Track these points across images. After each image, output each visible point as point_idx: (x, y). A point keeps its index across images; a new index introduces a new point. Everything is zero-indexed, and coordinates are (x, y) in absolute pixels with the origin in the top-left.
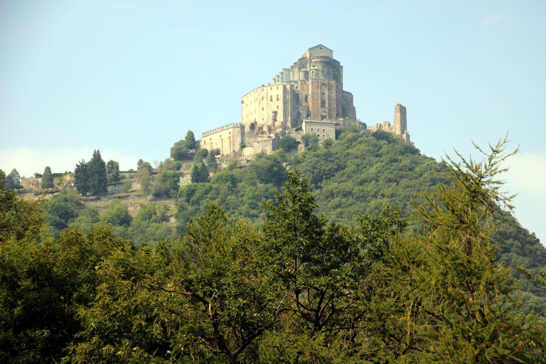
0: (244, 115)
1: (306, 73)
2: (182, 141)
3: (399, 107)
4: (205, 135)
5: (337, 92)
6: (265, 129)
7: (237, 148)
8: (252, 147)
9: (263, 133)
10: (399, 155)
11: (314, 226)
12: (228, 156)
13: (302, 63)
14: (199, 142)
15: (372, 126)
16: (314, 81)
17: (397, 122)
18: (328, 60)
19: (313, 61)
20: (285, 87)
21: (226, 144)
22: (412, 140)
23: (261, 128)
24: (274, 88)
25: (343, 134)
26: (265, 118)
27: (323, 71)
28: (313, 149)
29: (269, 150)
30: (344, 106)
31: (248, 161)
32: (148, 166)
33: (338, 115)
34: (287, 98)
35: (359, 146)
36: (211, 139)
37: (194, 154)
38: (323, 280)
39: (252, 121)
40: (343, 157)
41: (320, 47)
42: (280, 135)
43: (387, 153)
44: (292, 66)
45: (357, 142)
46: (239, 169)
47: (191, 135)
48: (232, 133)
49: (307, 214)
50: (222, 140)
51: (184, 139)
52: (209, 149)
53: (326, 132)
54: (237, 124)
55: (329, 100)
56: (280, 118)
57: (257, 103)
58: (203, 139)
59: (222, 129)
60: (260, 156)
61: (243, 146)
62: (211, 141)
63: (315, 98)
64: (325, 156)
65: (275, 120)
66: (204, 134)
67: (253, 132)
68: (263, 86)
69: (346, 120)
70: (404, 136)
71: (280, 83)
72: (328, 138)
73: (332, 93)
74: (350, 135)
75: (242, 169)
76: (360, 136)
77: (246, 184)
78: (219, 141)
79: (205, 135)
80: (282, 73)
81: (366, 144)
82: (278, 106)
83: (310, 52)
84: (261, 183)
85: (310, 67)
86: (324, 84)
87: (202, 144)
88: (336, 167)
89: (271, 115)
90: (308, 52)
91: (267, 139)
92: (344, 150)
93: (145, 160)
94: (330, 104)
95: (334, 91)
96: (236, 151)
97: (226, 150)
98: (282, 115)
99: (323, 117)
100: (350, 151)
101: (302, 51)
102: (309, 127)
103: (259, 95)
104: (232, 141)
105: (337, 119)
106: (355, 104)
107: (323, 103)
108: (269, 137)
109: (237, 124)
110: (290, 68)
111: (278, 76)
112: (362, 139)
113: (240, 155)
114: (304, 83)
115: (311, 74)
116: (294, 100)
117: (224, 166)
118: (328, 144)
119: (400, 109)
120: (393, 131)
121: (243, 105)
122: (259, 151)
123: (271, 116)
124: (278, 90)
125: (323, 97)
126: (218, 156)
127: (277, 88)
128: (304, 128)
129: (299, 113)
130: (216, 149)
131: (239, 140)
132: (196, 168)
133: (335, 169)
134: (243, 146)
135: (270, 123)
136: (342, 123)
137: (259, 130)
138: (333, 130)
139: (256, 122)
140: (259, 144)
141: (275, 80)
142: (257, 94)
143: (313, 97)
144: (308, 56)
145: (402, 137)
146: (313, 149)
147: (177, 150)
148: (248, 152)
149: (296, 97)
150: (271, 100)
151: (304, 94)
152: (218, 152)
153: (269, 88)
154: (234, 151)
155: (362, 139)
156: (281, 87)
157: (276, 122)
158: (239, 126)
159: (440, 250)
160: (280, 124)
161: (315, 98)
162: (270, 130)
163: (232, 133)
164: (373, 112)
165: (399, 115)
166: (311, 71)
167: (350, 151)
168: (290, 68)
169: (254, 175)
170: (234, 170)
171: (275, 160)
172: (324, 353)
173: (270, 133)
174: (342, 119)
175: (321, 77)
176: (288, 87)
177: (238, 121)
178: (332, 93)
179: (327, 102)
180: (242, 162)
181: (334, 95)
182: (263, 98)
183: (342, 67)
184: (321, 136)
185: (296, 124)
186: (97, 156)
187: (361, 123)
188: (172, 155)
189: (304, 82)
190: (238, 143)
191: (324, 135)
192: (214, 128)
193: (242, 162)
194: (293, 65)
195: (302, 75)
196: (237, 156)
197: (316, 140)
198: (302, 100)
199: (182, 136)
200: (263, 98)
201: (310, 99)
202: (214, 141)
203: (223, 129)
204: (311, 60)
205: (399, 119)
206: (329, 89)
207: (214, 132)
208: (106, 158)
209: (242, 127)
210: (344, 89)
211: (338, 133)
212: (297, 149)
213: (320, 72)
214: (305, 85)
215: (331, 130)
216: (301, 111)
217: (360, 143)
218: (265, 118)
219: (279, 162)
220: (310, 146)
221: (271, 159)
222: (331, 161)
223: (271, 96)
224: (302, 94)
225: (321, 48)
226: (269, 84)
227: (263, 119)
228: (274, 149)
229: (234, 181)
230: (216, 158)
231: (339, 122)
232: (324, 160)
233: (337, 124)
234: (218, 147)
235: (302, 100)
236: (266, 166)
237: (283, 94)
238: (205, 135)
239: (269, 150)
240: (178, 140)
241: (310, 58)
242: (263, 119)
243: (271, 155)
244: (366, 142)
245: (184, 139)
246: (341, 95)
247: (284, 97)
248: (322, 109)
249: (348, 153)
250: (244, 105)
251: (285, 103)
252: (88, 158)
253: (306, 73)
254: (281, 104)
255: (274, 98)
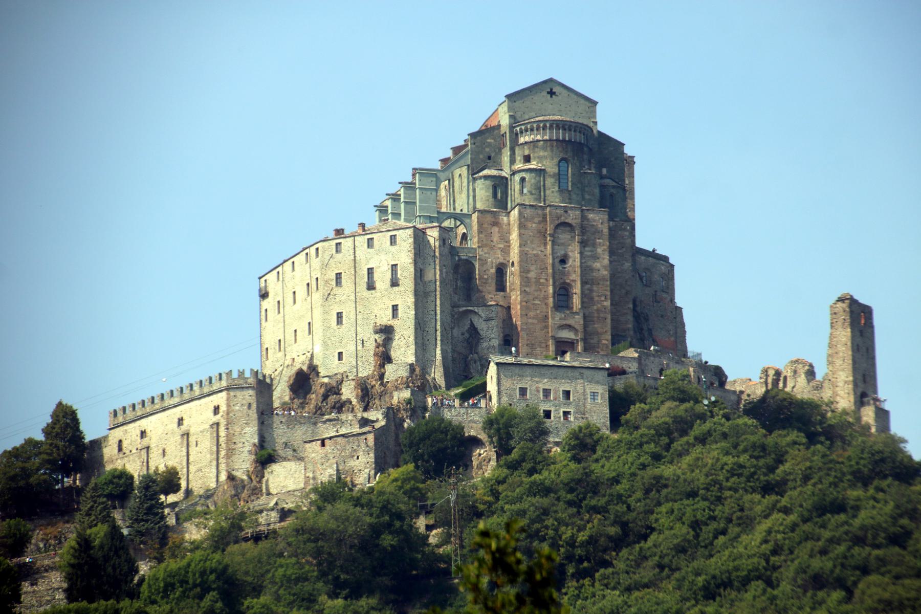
0: (270, 341)
2: (30, 442)
3: (845, 305)
4: (121, 417)
5: (612, 253)
6: (348, 392)
7: (243, 464)
8: (301, 459)
9: (340, 407)
10: (853, 486)
12: (209, 495)
13: (482, 148)
14: (97, 445)
16: (528, 212)
17: (838, 362)
18: (580, 138)
19: (522, 140)
20: (419, 237)
21: (203, 451)
22: (897, 428)
23: (333, 390)
24: (382, 240)
25: (636, 409)
26: (349, 349)
27: (559, 177)
28: (527, 466)
29: (362, 470)
31: (284, 514)
34: (429, 276)
35: (698, 450)
36: (143, 434)
37: (79, 491)
39: (301, 363)
40: (639, 494)
41: (550, 88)
42: (403, 414)
43: (806, 478)
44: (445, 161)
45: (691, 439)
46: (250, 544)
48: (223, 408)
50: (186, 435)
51: (40, 437)
53: (578, 401)
54: (241, 373)
55: (584, 283)
56: (404, 351)
57: (317, 296)
58: (117, 434)
59: (187, 396)
61: (265, 458)
62: (146, 442)
63: (532, 275)
64: (571, 491)
65: (385, 358)
66: (115, 413)
67: (302, 406)
68: (339, 232)
69: (648, 355)
70: (868, 415)
71: (402, 223)
72: (581, 423)
75: (262, 544)
76: (702, 417)
77: (278, 598)
79: (120, 419)
80: (409, 186)
81: (723, 444)
82: (395, 308)
83: (510, 109)
84: (333, 595)
85: (513, 161)
87: (109, 451)
88: (613, 530)
89: (372, 339)
90: (505, 108)
91: (356, 429)
92: (644, 467)
94: (587, 298)
96: (241, 475)
97: (203, 475)
98: (412, 340)
100: (667, 470)
101: (485, 105)
102: (513, 384)
104: (222, 440)
105: (615, 352)
108: (364, 422)
109: (241, 373)
110: (438, 166)
111: (395, 197)
112: (708, 425)
113: (256, 492)
115: (517, 187)
117: (194, 533)
118: (583, 444)
119: (852, 313)
120: (826, 394)
121: (266, 304)
122: (326, 474)
123: (371, 346)
124: (393, 248)
125: (563, 273)
126: (172, 498)
127: (393, 241)
128: (492, 387)
130: (162, 468)
131: (249, 435)
133: (610, 538)
134: (265, 458)
135: (367, 369)
136: (634, 367)
137: (325, 397)
138: (602, 391)
139: (313, 368)
140: (327, 448)
141: (382, 210)
142: (315, 262)
143: (524, 271)
144: (504, 120)
145: (859, 419)
146: (527, 466)
147: (13, 478)
148: (286, 480)
150: (371, 287)
153: (362, 241)
154: (231, 478)
155: (708, 425)
156: (406, 238)
157: (388, 367)
158: (252, 381)
160: (404, 373)
161: (532, 275)
162: (366, 395)
163: (223, 408)
165: (845, 335)
166: (517, 178)
168: (438, 166)
170: (233, 548)
171: (385, 508)
173: (366, 409)
174: (632, 353)
175: (553, 197)
178: (596, 258)
179: (577, 289)
180: (262, 519)
181: (602, 264)
182: (338, 276)
183: (631, 161)
184: (557, 415)
185: (465, 374)
187: (703, 367)
189: (489, 218)
190: (248, 447)
191: (566, 414)
192: (156, 393)
193: (262, 519)
194: (449, 154)
195: (483, 191)
196: (245, 495)
197: (540, 433)
200: (338, 276)
201: (513, 278)
202: (153, 440)
203: (189, 394)
205: (845, 351)
206: (583, 244)
207: (155, 405)
209: (263, 387)
210: (639, 243)
211: (619, 405)
212: (468, 465)
213: (550, 181)
214: (495, 229)
215: (594, 395)
216: (480, 325)
217: (702, 440)
218: (349, 349)
219: (400, 516)
220: (515, 455)
221: (370, 505)
222: (595, 510)
223: (370, 271)
224: (483, 262)
225: (551, 93)
226: (362, 225)
228: (380, 466)
230: (162, 506)
231: (625, 365)
232: (570, 503)
233: (614, 373)
234: (170, 464)
236: (351, 530)
237: (415, 263)
238: (121, 417)
239: (362, 470)
241: (511, 127)
242: (340, 354)
243: (372, 489)
244: (725, 436)
245: (40, 437)
246: (627, 265)
247: (419, 275)
248: (558, 315)
249: (658, 478)
250: (267, 304)
251: (421, 294)
253: (500, 186)
254: (405, 298)
255: (382, 279)
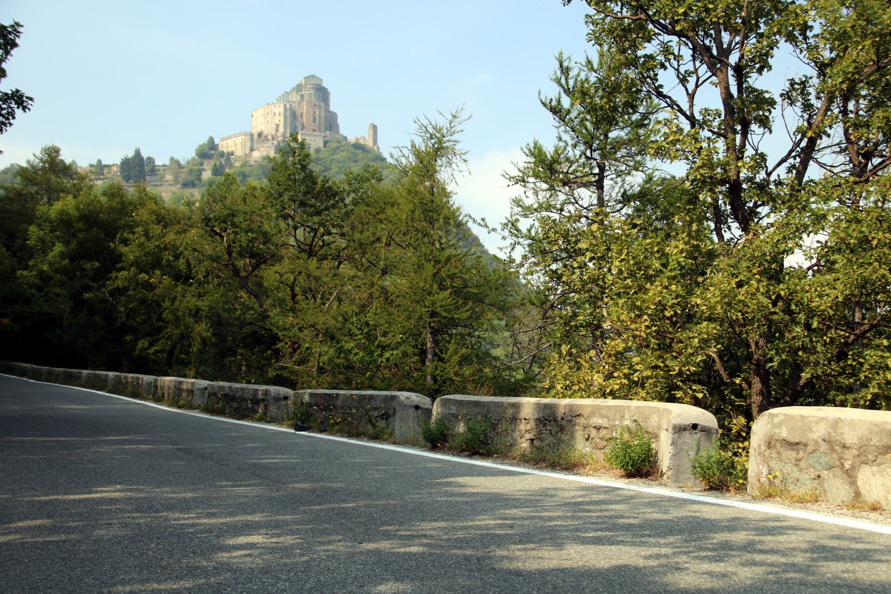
1: (302, 96)
4: (223, 140)
7: (248, 151)
11: (310, 178)
13: (299, 88)
15: (351, 139)
20: (285, 106)
21: (239, 148)
22: (381, 151)
23: (266, 137)
24: (277, 106)
29: (272, 154)
30: (330, 122)
32: (178, 162)
33: (326, 130)
38: (316, 219)
39: (260, 130)
41: (313, 76)
47: (211, 140)
49: (304, 168)
52: (225, 151)
56: (281, 130)
60: (264, 158)
61: (252, 150)
65: (277, 131)
70: (375, 148)
74: (334, 145)
78: (234, 146)
87: (220, 146)
89: (275, 127)
93: (175, 157)
95: (323, 110)
97: (239, 152)
99: (314, 130)
100: (335, 157)
101: (299, 79)
106: (339, 121)
107: (315, 120)
114: (300, 103)
116: (292, 116)
117: (237, 164)
118: (318, 151)
122: (265, 154)
129: (296, 127)
131: (249, 145)
132: (215, 165)
134: (252, 150)
135: (273, 133)
148: (256, 155)
151: (300, 112)
152: (232, 154)
156: (282, 106)
159: (409, 192)
162: (273, 138)
164: (352, 129)
165: (372, 131)
167: (335, 157)
169: (260, 172)
172: (317, 273)
175: (313, 99)
176: (288, 106)
177: (248, 130)
181: (323, 114)
186: (138, 153)
188: (197, 154)
195: (299, 98)
199: (205, 140)
201: (304, 115)
203: (236, 136)
205: (371, 135)
207: (230, 137)
208: (145, 155)
209: (252, 135)
211: (325, 143)
227: (268, 129)
229: (244, 176)
238: (223, 140)
240: (201, 143)
251: (285, 117)
252: (131, 154)
253: (302, 96)
254: (282, 119)
255: (277, 114)
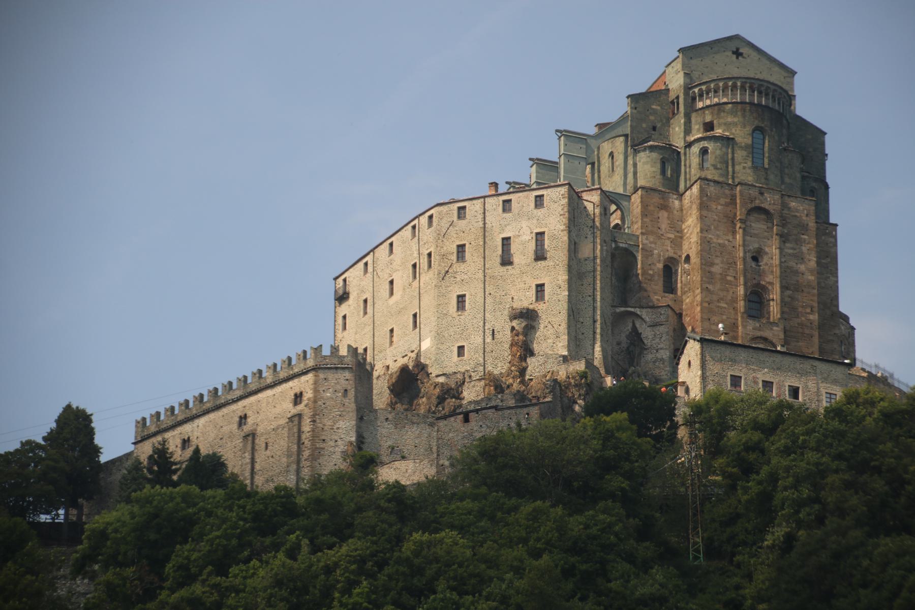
1: (670, 159)
16: (712, 189)
27: (753, 150)
41: (736, 46)
48: (308, 395)
55: (784, 288)
57: (427, 277)
63: (717, 269)
65: (524, 350)
73: (801, 259)
82: (540, 288)
85: (688, 131)
86: (760, 210)
90: (678, 65)
94: (788, 307)
98: (563, 328)
103: (442, 236)
107: (756, 299)
115: (695, 160)
124: (540, 212)
125: (760, 273)
129: (636, 337)
135: (500, 366)
137: (441, 400)
139: (421, 367)
143: (706, 264)
144: (676, 81)
149: (621, 261)
150: (506, 261)
151: (662, 251)
153: (495, 204)
158: (349, 360)
161: (717, 269)
163: (308, 395)
166: (695, 149)
175: (744, 172)
178: (801, 259)
179: (775, 294)
182: (461, 248)
189: (656, 199)
190: (341, 447)
198: (651, 279)
200: (461, 248)
201: (689, 277)
204: (691, 100)
206: (784, 238)
213: (740, 154)
214: (664, 214)
216: (647, 333)
223: (506, 241)
224: (648, 253)
225: (737, 53)
235: (651, 279)
241: (687, 88)
242: (461, 349)
247: (573, 248)
248: (752, 324)
251: (577, 273)
253: (670, 159)
254: (555, 277)
255: (522, 252)
